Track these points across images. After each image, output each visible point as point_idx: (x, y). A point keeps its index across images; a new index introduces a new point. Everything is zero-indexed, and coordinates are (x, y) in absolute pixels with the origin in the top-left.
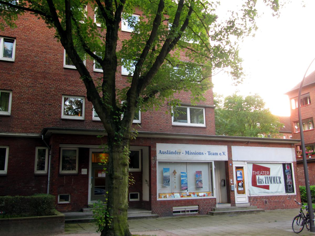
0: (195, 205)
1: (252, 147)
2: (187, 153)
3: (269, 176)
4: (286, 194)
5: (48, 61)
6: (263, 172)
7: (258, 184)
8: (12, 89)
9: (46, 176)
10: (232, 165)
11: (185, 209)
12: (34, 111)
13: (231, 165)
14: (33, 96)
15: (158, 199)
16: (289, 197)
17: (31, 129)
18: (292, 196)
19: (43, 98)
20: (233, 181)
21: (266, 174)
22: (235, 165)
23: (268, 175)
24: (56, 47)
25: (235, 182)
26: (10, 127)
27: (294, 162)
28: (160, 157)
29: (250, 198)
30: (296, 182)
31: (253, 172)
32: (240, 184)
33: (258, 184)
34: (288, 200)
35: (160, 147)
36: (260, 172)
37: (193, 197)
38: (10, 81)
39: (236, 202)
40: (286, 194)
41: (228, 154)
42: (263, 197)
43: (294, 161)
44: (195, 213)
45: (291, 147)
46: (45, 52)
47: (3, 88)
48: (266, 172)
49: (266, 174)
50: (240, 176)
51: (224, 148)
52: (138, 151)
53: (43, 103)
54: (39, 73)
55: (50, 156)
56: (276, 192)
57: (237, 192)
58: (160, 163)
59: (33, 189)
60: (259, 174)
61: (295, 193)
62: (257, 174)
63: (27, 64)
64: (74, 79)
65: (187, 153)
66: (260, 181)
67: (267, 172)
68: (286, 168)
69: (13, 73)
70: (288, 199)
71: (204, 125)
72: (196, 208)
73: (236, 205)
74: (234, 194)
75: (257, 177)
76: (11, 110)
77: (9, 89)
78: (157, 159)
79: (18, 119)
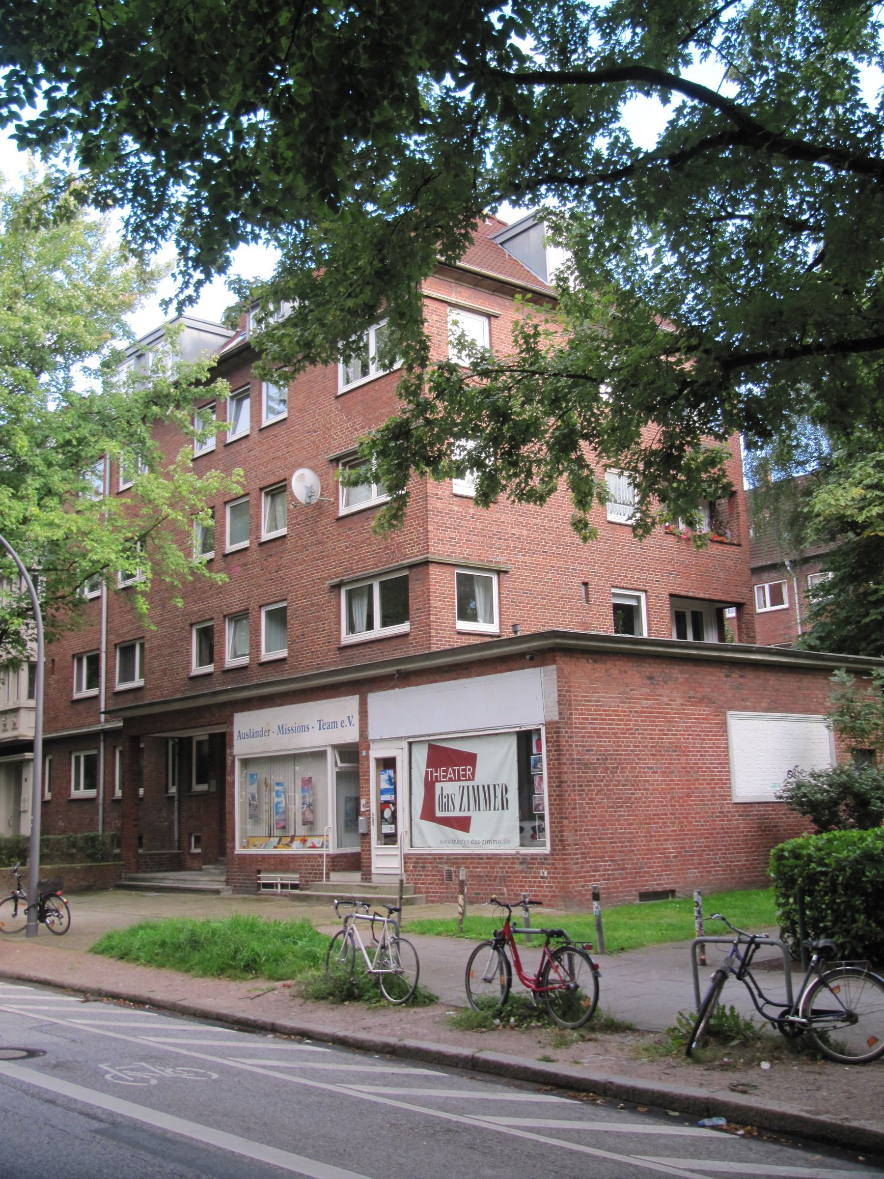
0: (294, 871)
2: (281, 729)
3: (470, 783)
6: (454, 771)
7: (439, 814)
10: (368, 754)
13: (364, 753)
16: (521, 863)
18: (534, 857)
20: (368, 803)
21: (464, 776)
22: (377, 752)
23: (469, 779)
25: (374, 810)
27: (548, 725)
28: (241, 748)
29: (407, 858)
30: (550, 805)
31: (427, 772)
32: (387, 814)
33: (439, 814)
34: (521, 872)
36: (446, 771)
37: (296, 849)
39: (374, 871)
43: (549, 719)
45: (542, 664)
48: (464, 770)
49: (464, 776)
51: (350, 704)
56: (489, 842)
57: (379, 839)
58: (245, 762)
60: (444, 777)
62: (437, 781)
65: (281, 729)
66: (445, 800)
68: (535, 751)
70: (519, 867)
73: (374, 878)
74: (370, 843)
75: (438, 786)
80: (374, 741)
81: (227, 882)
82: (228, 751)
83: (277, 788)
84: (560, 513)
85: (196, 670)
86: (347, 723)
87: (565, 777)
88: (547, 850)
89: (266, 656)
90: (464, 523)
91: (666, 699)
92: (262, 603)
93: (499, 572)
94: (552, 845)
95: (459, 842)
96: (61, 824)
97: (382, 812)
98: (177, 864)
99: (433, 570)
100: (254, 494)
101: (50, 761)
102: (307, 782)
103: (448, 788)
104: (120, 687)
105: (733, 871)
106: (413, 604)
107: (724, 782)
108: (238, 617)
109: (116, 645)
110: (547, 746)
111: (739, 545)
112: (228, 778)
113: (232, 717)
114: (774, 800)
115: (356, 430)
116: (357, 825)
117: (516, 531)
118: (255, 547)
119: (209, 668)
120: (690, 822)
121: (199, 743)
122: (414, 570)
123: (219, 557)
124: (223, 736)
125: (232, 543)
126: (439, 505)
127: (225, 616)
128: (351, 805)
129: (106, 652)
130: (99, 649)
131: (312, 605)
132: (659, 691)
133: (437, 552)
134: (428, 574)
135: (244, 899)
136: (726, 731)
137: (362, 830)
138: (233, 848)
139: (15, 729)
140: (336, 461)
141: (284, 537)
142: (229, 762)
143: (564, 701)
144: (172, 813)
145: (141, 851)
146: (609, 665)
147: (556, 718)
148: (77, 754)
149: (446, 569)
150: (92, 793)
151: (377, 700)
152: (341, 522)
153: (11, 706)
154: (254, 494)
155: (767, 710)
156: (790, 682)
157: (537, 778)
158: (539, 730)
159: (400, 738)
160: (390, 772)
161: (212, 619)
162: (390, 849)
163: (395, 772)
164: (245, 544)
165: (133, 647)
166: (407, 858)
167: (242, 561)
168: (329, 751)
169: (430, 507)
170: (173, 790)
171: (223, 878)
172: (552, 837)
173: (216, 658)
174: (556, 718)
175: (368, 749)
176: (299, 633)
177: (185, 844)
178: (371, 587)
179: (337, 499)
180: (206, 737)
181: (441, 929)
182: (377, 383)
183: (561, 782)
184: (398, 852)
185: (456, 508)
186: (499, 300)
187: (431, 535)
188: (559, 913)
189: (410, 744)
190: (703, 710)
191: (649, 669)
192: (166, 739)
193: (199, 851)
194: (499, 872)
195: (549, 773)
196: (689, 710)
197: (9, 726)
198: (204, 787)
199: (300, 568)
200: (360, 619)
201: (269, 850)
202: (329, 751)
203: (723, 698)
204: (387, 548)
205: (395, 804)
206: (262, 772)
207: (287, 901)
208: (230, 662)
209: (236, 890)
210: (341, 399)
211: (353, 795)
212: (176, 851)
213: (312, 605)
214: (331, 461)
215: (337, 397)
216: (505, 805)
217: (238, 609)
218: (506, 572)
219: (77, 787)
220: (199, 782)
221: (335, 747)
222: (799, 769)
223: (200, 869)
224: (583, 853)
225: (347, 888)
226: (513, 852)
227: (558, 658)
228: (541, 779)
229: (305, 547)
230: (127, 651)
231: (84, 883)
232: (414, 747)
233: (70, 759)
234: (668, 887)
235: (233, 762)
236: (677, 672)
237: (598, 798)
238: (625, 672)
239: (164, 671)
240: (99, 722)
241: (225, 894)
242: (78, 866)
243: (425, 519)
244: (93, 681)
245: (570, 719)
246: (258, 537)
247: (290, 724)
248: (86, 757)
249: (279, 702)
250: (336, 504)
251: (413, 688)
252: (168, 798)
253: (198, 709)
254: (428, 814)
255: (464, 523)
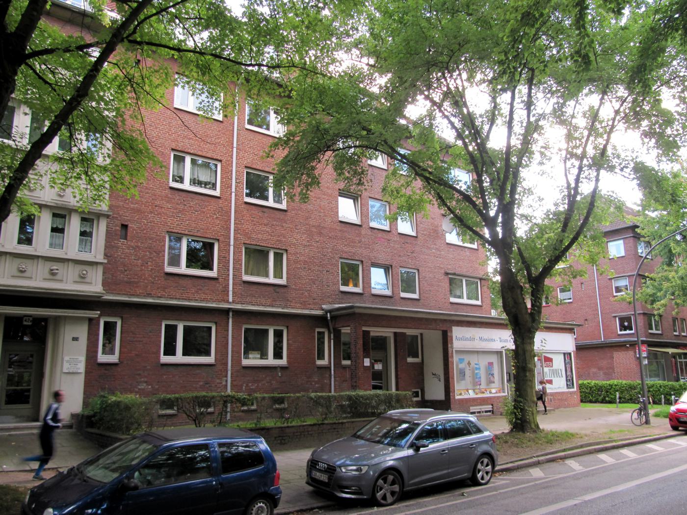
2: (481, 339)
4: (568, 390)
5: (322, 211)
8: (287, 248)
9: (328, 368)
11: (480, 409)
12: (312, 279)
14: (310, 259)
15: (457, 397)
17: (309, 304)
18: (573, 392)
19: (321, 262)
24: (330, 191)
26: (288, 300)
27: (573, 351)
37: (487, 395)
38: (284, 237)
40: (568, 390)
44: (489, 413)
46: (319, 198)
47: (278, 247)
52: (417, 336)
53: (320, 269)
54: (313, 226)
55: (332, 341)
59: (317, 385)
61: (575, 389)
63: (301, 213)
64: (350, 237)
65: (481, 339)
69: (287, 225)
70: (569, 395)
71: (479, 303)
72: (489, 407)
76: (287, 278)
77: (284, 248)
78: (454, 346)
79: (295, 289)
82: (449, 345)
194: (564, 398)
201: (472, 394)
233: (161, 325)
247: (485, 337)
248: (187, 331)
249: (479, 326)
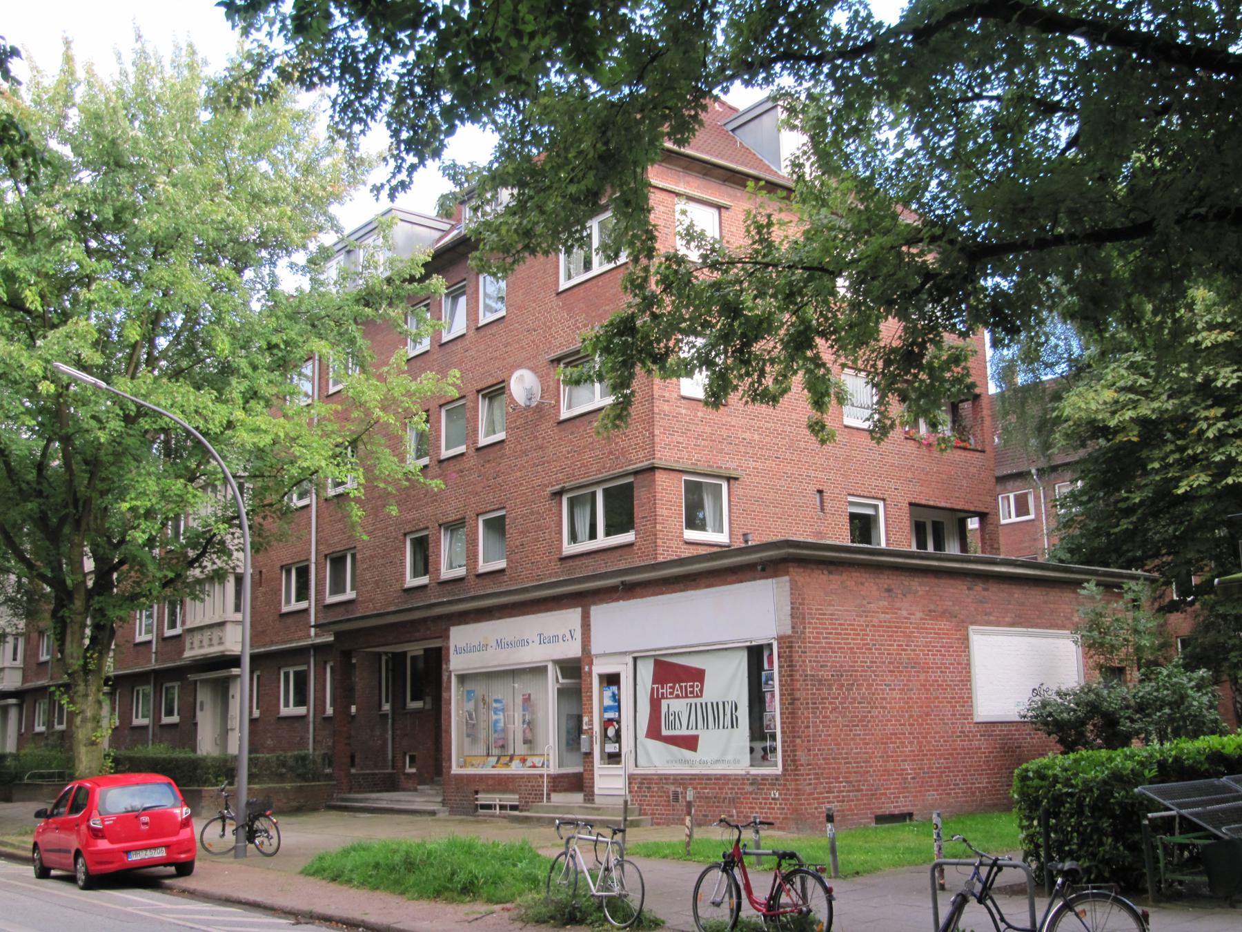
0: (513, 792)
1: (645, 600)
3: (698, 700)
7: (665, 732)
10: (590, 669)
13: (587, 668)
16: (752, 784)
18: (764, 778)
20: (591, 721)
21: (692, 692)
22: (600, 667)
23: (697, 696)
25: (597, 728)
27: (780, 639)
28: (457, 663)
29: (631, 778)
30: (782, 723)
31: (653, 689)
33: (665, 732)
35: (460, 636)
37: (515, 768)
39: (596, 791)
41: (583, 634)
42: (665, 778)
43: (781, 633)
45: (775, 575)
49: (692, 692)
50: (611, 703)
51: (573, 616)
56: (718, 761)
58: (462, 678)
60: (671, 693)
62: (663, 697)
66: (671, 718)
67: (692, 687)
68: (766, 666)
70: (749, 788)
73: (597, 799)
74: (592, 762)
75: (664, 703)
80: (597, 656)
81: (444, 803)
82: (444, 666)
83: (495, 705)
84: (794, 416)
85: (410, 581)
86: (568, 636)
87: (798, 694)
88: (778, 770)
89: (483, 567)
90: (692, 427)
91: (904, 613)
92: (480, 511)
93: (729, 479)
94: (784, 766)
95: (687, 762)
96: (269, 742)
97: (606, 730)
98: (391, 784)
99: (660, 477)
100: (471, 397)
101: (258, 677)
102: (527, 699)
103: (675, 706)
104: (331, 600)
105: (973, 793)
106: (638, 513)
107: (966, 700)
108: (453, 526)
109: (326, 556)
110: (780, 662)
111: (983, 451)
112: (445, 695)
113: (447, 630)
114: (1018, 719)
115: (578, 328)
116: (579, 744)
117: (747, 435)
118: (472, 452)
119: (424, 580)
120: (929, 742)
121: (414, 658)
122: (640, 477)
123: (434, 463)
124: (439, 650)
125: (447, 449)
126: (666, 408)
127: (440, 526)
128: (573, 723)
129: (316, 563)
130: (308, 560)
131: (532, 513)
132: (898, 605)
133: (663, 457)
134: (654, 481)
135: (461, 821)
136: (968, 647)
137: (584, 749)
138: (450, 767)
139: (221, 643)
140: (557, 361)
141: (502, 442)
142: (445, 678)
143: (797, 615)
144: (385, 731)
145: (353, 771)
146: (844, 577)
147: (789, 632)
148: (286, 669)
149: (673, 475)
150: (302, 710)
151: (601, 614)
152: (563, 426)
153: (217, 620)
154: (471, 397)
155: (1012, 625)
156: (1036, 596)
157: (768, 696)
158: (770, 646)
159: (624, 653)
160: (614, 689)
161: (427, 528)
162: (613, 769)
163: (619, 689)
164: (461, 449)
165: (344, 558)
166: (631, 778)
167: (458, 467)
168: (550, 667)
169: (656, 410)
170: (387, 707)
171: (440, 799)
172: (783, 756)
173: (431, 569)
174: (789, 632)
175: (591, 664)
176: (518, 543)
177: (400, 764)
178: (594, 494)
179: (558, 401)
180: (422, 652)
181: (667, 852)
182: (600, 279)
183: (794, 699)
184: (622, 772)
185: (684, 411)
186: (730, 190)
187: (657, 440)
188: (791, 836)
189: (635, 659)
190: (944, 625)
191: (890, 581)
192: (379, 655)
193: (413, 770)
194: (728, 793)
195: (781, 690)
196: (929, 623)
197: (215, 641)
198: (418, 705)
199: (519, 474)
200: (583, 528)
201: (488, 769)
202: (550, 667)
203: (964, 612)
204: (611, 453)
205: (619, 722)
206: (480, 688)
207: (505, 823)
208: (446, 573)
209: (453, 812)
210: (563, 295)
211: (575, 712)
212: (390, 771)
213: (532, 513)
214: (552, 361)
215: (558, 294)
216: (734, 723)
217: (454, 518)
218: (736, 479)
219: (287, 705)
220: (413, 699)
221: (556, 662)
222: (1044, 687)
223: (416, 790)
224: (816, 774)
225: (569, 810)
226: (743, 772)
227: (791, 569)
228: (773, 696)
229: (525, 453)
230: (338, 562)
231: (294, 804)
232: (639, 663)
234: (905, 810)
235: (449, 678)
236: (918, 585)
237: (832, 717)
238: (862, 584)
239: (376, 583)
240: (309, 636)
241: (441, 816)
242: (288, 786)
243: (651, 422)
244: (302, 594)
245: (803, 633)
246: (476, 442)
247: (509, 639)
248: (296, 673)
250: (557, 407)
251: (639, 600)
252: (382, 716)
253: (413, 623)
254: (654, 732)
255: (692, 427)
